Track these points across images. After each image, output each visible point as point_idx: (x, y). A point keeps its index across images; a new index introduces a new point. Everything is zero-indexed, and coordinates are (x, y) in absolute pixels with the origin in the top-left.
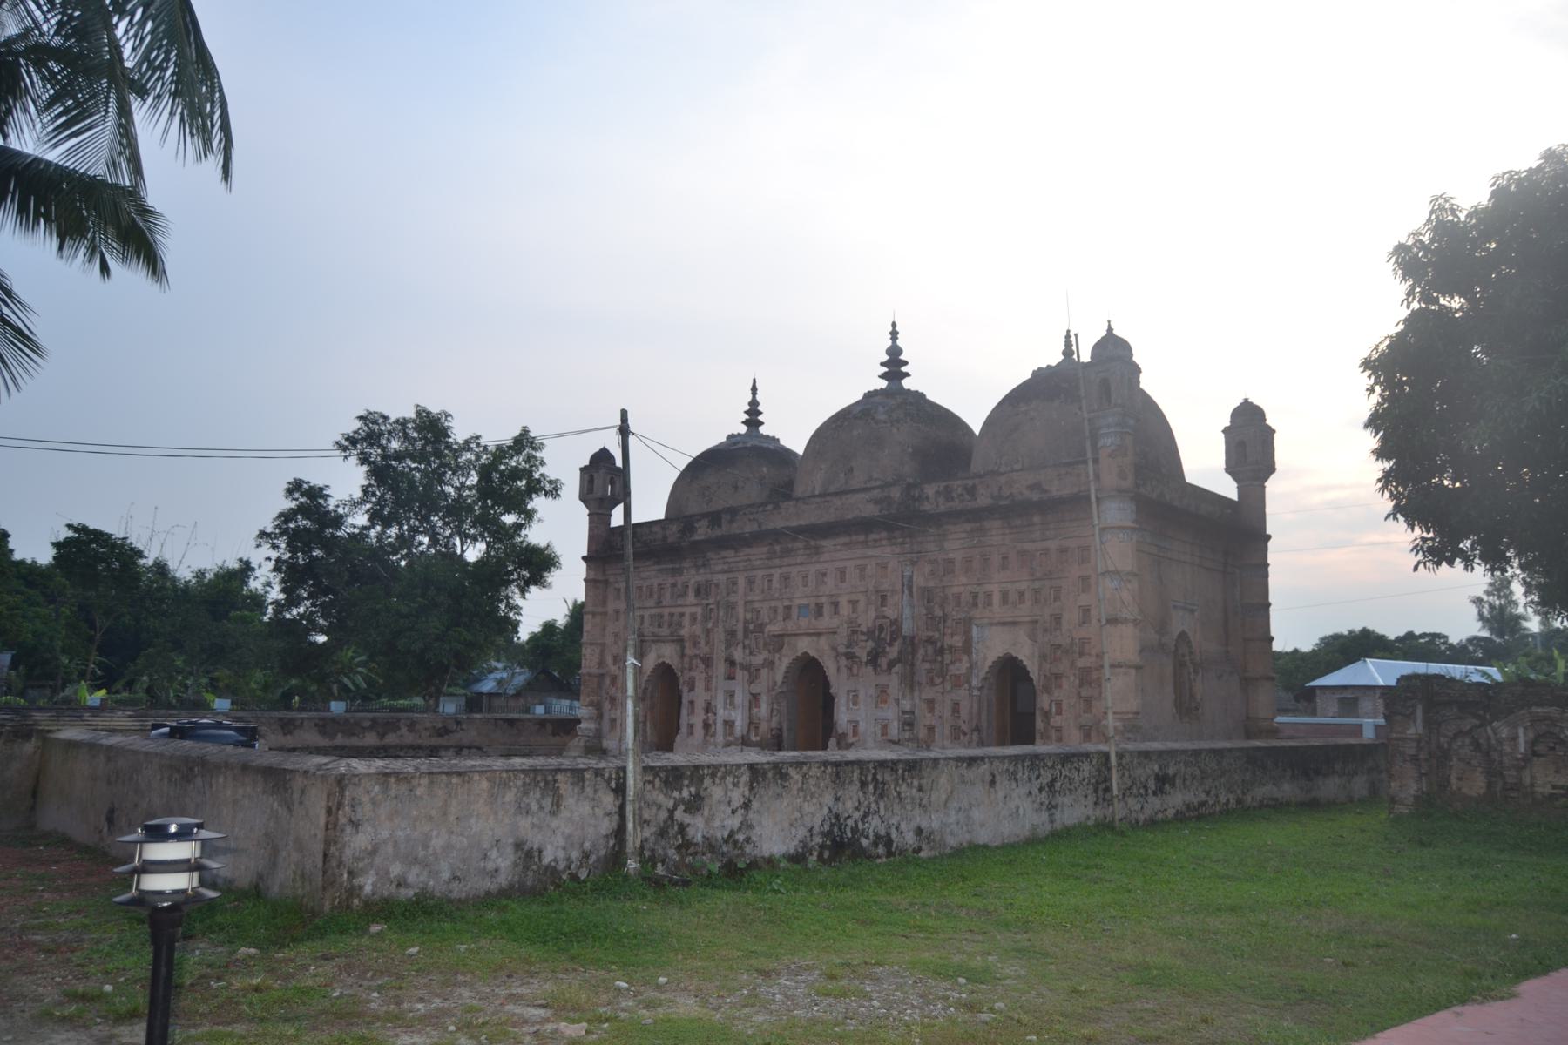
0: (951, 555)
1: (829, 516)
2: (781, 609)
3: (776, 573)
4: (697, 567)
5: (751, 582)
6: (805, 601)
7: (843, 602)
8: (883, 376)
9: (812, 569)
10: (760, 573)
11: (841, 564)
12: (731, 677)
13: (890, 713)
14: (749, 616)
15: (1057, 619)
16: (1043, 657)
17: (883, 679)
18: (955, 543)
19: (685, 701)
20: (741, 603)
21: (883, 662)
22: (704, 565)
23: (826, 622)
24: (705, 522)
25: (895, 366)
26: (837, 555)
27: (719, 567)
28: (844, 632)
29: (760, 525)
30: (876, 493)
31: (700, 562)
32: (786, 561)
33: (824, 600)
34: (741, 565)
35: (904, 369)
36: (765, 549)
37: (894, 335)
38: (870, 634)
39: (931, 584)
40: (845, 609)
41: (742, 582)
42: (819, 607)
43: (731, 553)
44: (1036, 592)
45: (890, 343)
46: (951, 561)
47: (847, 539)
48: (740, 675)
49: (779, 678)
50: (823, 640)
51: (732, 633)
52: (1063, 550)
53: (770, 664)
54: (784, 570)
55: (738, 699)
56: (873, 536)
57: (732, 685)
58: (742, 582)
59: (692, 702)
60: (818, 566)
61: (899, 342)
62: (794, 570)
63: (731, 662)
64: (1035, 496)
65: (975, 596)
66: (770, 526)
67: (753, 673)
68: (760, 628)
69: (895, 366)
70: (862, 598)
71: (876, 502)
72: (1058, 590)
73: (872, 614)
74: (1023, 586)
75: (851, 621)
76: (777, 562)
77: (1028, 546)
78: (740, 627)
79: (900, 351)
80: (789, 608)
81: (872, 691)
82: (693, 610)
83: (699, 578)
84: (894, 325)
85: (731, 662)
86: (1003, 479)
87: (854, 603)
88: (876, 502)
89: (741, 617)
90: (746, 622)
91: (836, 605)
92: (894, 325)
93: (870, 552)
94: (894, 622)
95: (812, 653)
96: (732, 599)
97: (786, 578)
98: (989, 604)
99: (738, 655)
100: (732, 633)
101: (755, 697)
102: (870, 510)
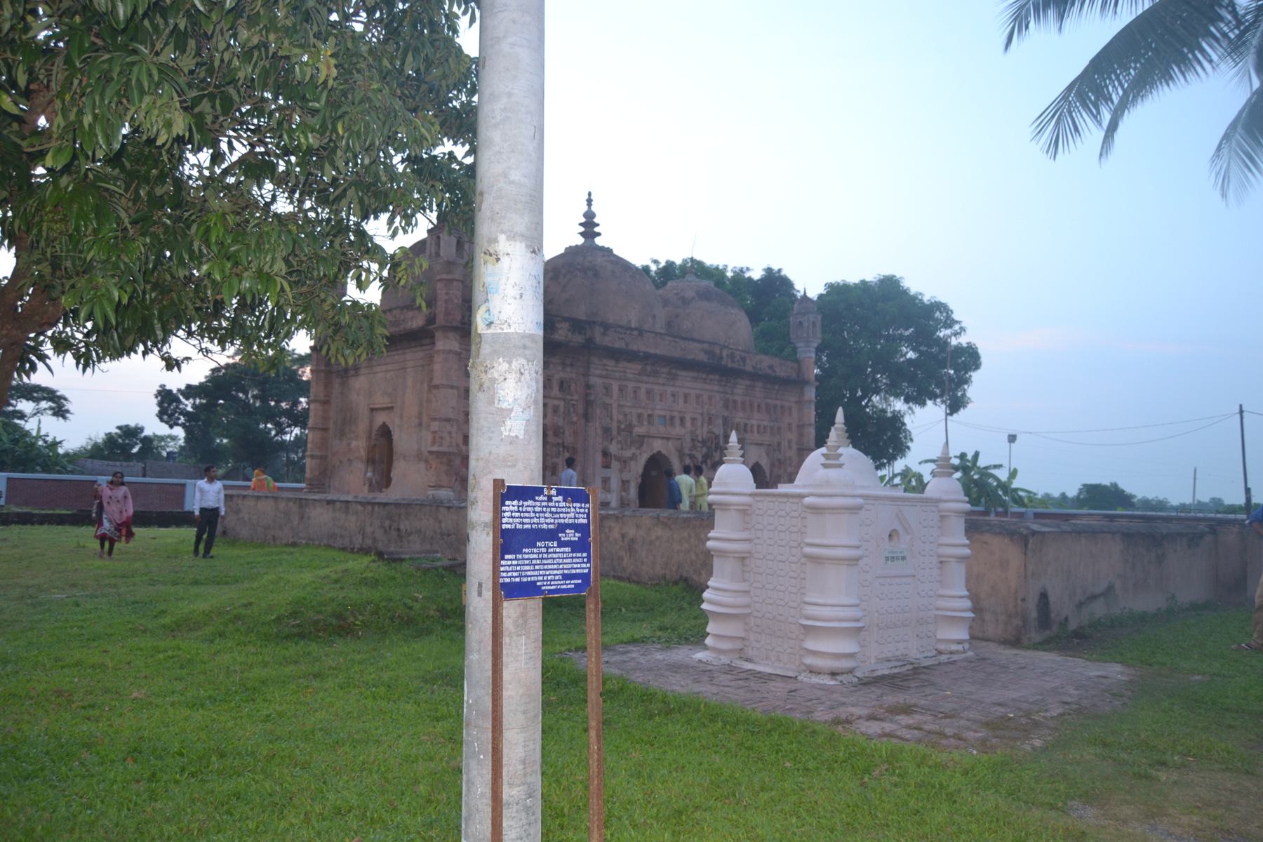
0: (736, 398)
1: (676, 353)
2: (646, 416)
3: (644, 387)
4: (564, 365)
5: (621, 390)
6: (662, 413)
7: (688, 417)
8: (582, 234)
9: (670, 389)
10: (631, 385)
11: (687, 391)
12: (607, 466)
14: (621, 417)
15: (779, 444)
16: (772, 465)
18: (739, 390)
20: (615, 406)
21: (709, 462)
22: (572, 365)
23: (677, 430)
24: (566, 325)
25: (589, 227)
26: (688, 384)
27: (598, 372)
28: (688, 439)
29: (627, 344)
30: (705, 346)
31: (568, 361)
32: (651, 379)
33: (675, 414)
34: (617, 375)
35: (582, 229)
36: (639, 367)
37: (589, 202)
38: (704, 442)
39: (726, 414)
40: (688, 423)
41: (615, 388)
42: (672, 418)
43: (612, 363)
44: (772, 428)
45: (586, 208)
46: (735, 402)
47: (695, 374)
48: (615, 465)
49: (641, 470)
50: (670, 443)
51: (607, 431)
52: (782, 407)
54: (649, 386)
55: (615, 484)
56: (711, 376)
57: (607, 472)
58: (615, 388)
60: (673, 389)
61: (593, 208)
62: (657, 388)
63: (606, 454)
64: (770, 372)
65: (746, 425)
66: (635, 348)
67: (624, 462)
68: (630, 427)
69: (589, 227)
70: (699, 417)
71: (707, 352)
72: (779, 428)
73: (705, 429)
74: (766, 423)
75: (692, 433)
76: (645, 378)
77: (769, 401)
78: (614, 425)
80: (649, 416)
82: (556, 402)
83: (562, 375)
84: (590, 194)
85: (606, 454)
86: (758, 357)
87: (693, 420)
88: (707, 352)
89: (615, 417)
90: (619, 422)
91: (682, 420)
92: (590, 194)
93: (706, 387)
94: (717, 437)
95: (664, 452)
96: (607, 400)
97: (648, 392)
98: (752, 431)
99: (613, 448)
100: (607, 431)
101: (625, 484)
102: (702, 357)
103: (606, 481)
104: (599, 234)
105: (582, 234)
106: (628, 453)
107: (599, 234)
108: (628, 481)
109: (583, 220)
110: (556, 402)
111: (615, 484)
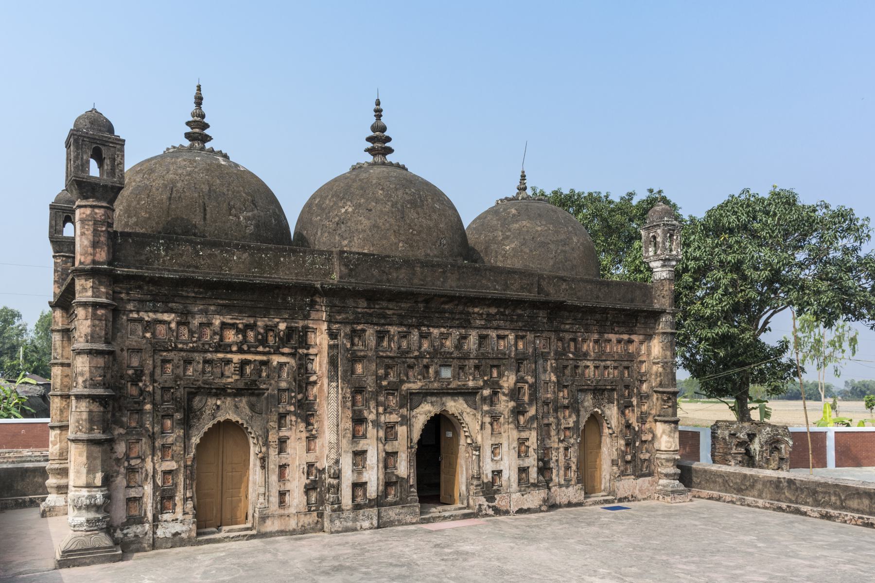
5: (381, 336)
8: (368, 150)
13: (531, 461)
17: (524, 435)
19: (273, 466)
21: (522, 419)
37: (378, 113)
41: (370, 333)
45: (373, 120)
53: (406, 421)
55: (372, 458)
59: (283, 467)
61: (383, 120)
69: (379, 142)
79: (383, 129)
81: (515, 444)
82: (283, 359)
84: (378, 103)
85: (358, 420)
92: (378, 103)
103: (359, 455)
104: (390, 151)
105: (368, 150)
106: (394, 418)
107: (390, 151)
108: (397, 453)
109: (372, 134)
110: (283, 359)
111: (372, 458)
